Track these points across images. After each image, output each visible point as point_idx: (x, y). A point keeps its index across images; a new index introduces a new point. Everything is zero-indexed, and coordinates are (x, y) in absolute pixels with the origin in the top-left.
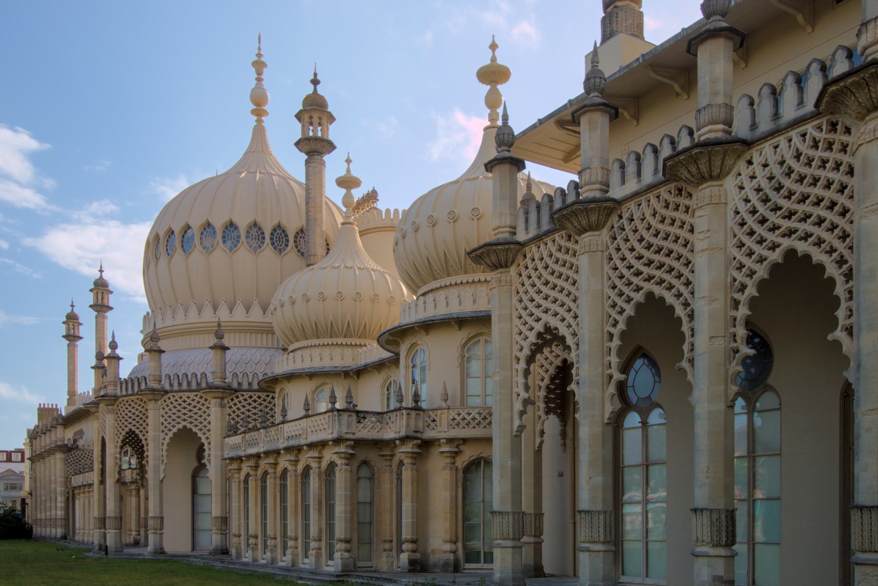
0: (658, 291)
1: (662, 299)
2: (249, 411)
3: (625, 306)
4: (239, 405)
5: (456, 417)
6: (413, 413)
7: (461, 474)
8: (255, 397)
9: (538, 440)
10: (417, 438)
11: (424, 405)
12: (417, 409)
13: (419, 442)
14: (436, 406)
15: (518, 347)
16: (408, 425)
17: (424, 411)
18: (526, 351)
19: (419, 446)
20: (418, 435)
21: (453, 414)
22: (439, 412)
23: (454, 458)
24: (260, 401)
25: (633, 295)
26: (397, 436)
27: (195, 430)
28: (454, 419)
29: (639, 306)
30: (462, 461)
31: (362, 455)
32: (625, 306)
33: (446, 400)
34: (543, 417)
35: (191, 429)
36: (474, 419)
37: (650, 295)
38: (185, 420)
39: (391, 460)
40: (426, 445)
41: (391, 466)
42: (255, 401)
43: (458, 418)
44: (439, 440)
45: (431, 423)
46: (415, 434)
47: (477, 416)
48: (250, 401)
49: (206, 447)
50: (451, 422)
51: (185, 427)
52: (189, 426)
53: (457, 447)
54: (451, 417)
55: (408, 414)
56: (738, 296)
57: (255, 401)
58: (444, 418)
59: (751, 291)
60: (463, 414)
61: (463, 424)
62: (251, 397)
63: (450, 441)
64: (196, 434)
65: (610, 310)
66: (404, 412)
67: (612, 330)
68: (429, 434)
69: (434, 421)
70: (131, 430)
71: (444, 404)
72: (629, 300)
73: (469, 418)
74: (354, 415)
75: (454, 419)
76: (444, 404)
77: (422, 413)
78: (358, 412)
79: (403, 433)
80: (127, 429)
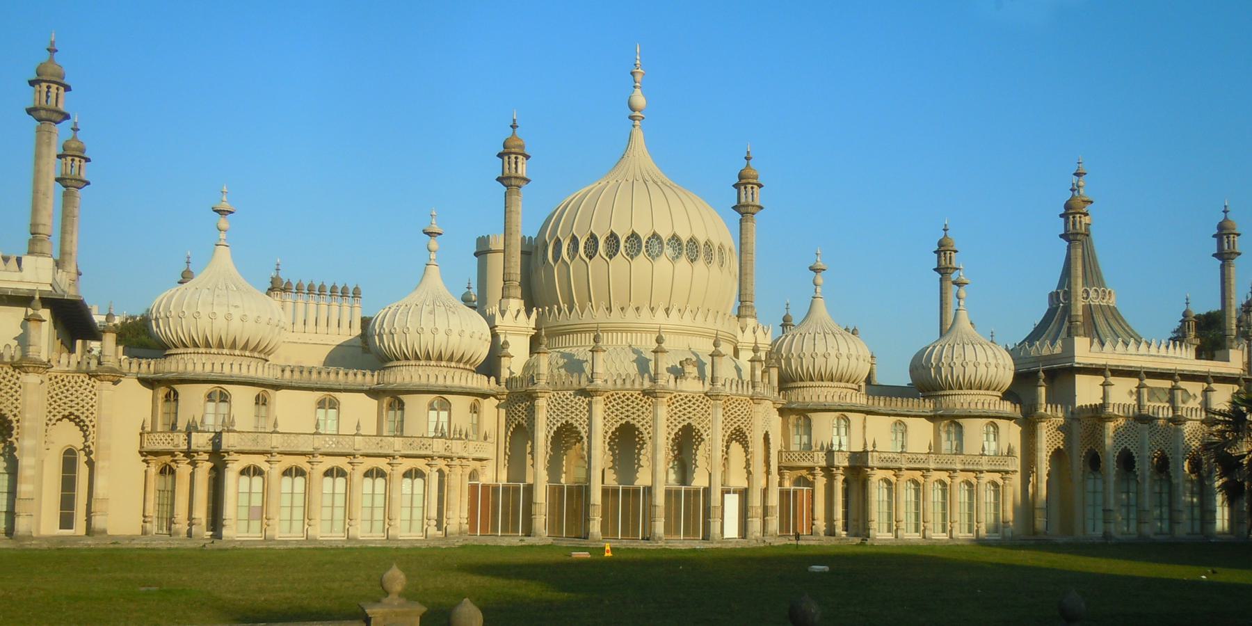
27: (576, 424)
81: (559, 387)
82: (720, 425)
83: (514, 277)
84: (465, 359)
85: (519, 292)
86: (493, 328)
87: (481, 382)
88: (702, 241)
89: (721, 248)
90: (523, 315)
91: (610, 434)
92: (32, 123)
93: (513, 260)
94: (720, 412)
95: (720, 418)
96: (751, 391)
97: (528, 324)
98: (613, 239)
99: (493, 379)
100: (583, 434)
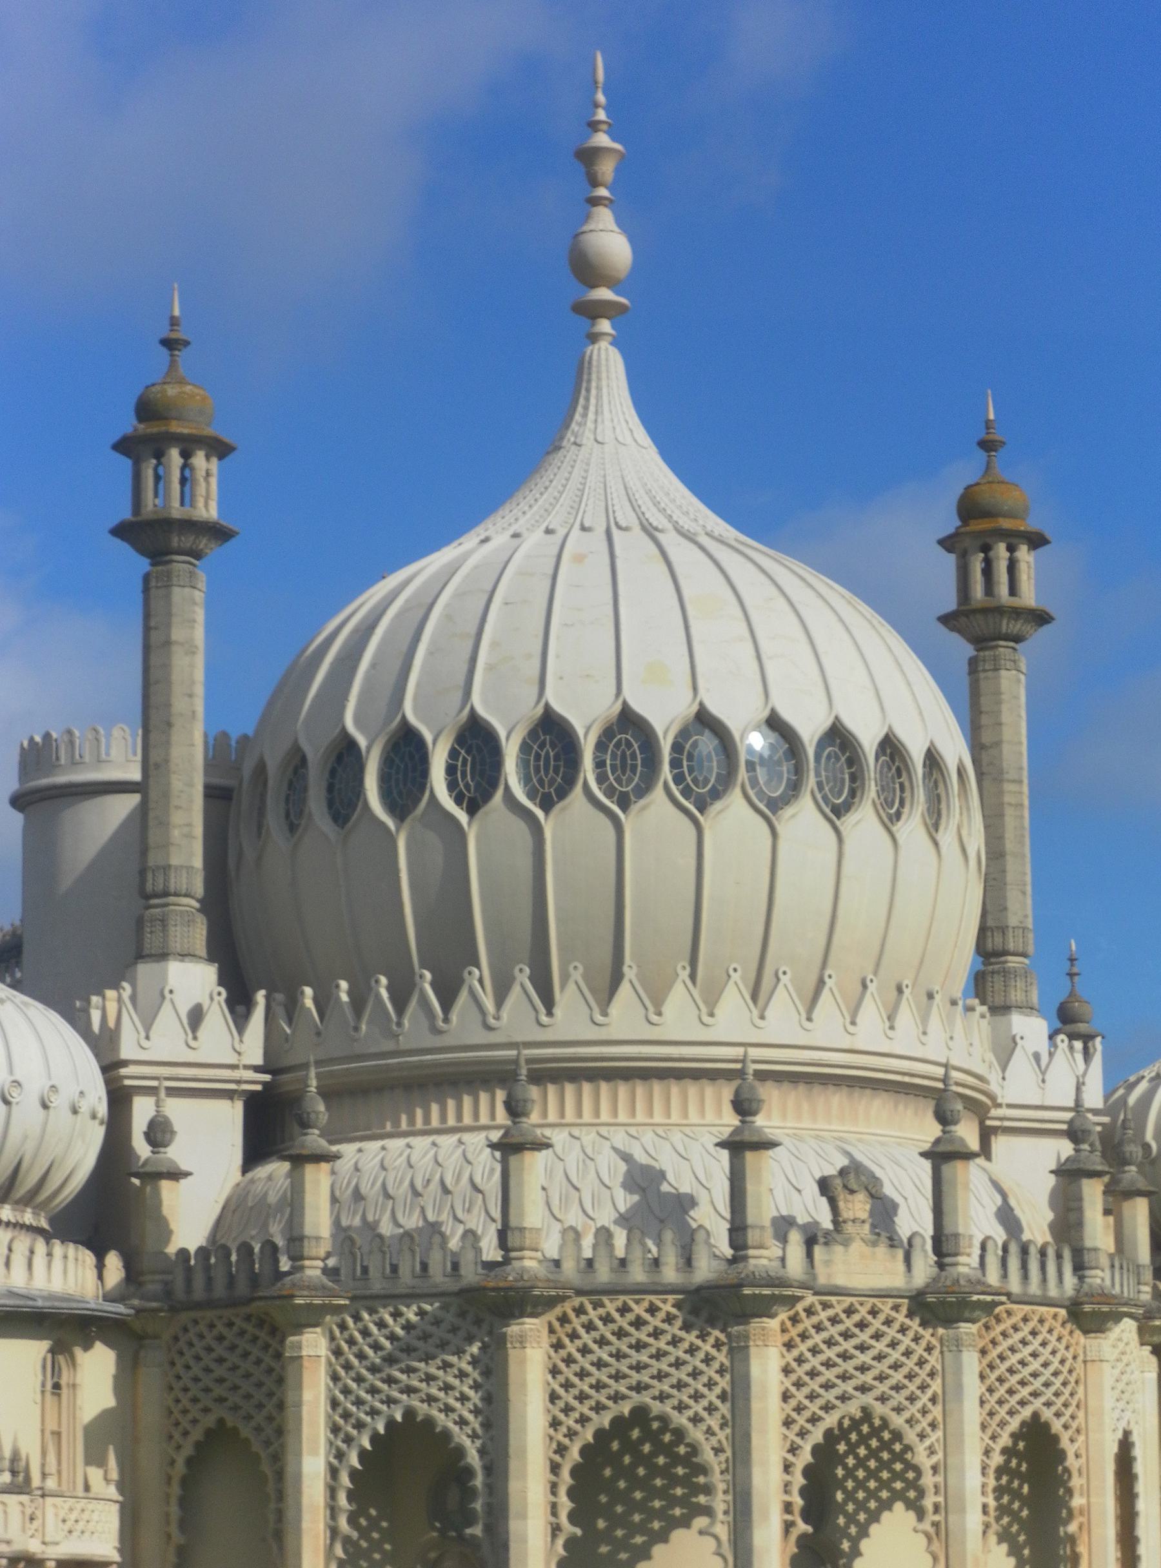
2: (619, 1356)
4: (587, 1338)
8: (639, 1310)
24: (656, 1322)
35: (429, 1422)
38: (409, 1390)
42: (638, 1323)
48: (623, 1322)
49: (479, 1481)
51: (409, 1413)
52: (422, 1409)
57: (638, 1323)
62: (624, 1310)
64: (446, 1435)
70: (221, 1422)
80: (209, 1421)
81: (377, 1285)
82: (971, 1414)
83: (177, 882)
84: (21, 1190)
85: (199, 934)
86: (110, 1068)
87: (71, 1276)
88: (868, 739)
89: (933, 759)
90: (217, 1018)
91: (574, 1454)
92: (164, 351)
93: (177, 818)
94: (971, 1363)
95: (973, 1388)
96: (1070, 1280)
97: (237, 1049)
98: (552, 735)
99: (114, 1262)
100: (473, 1458)
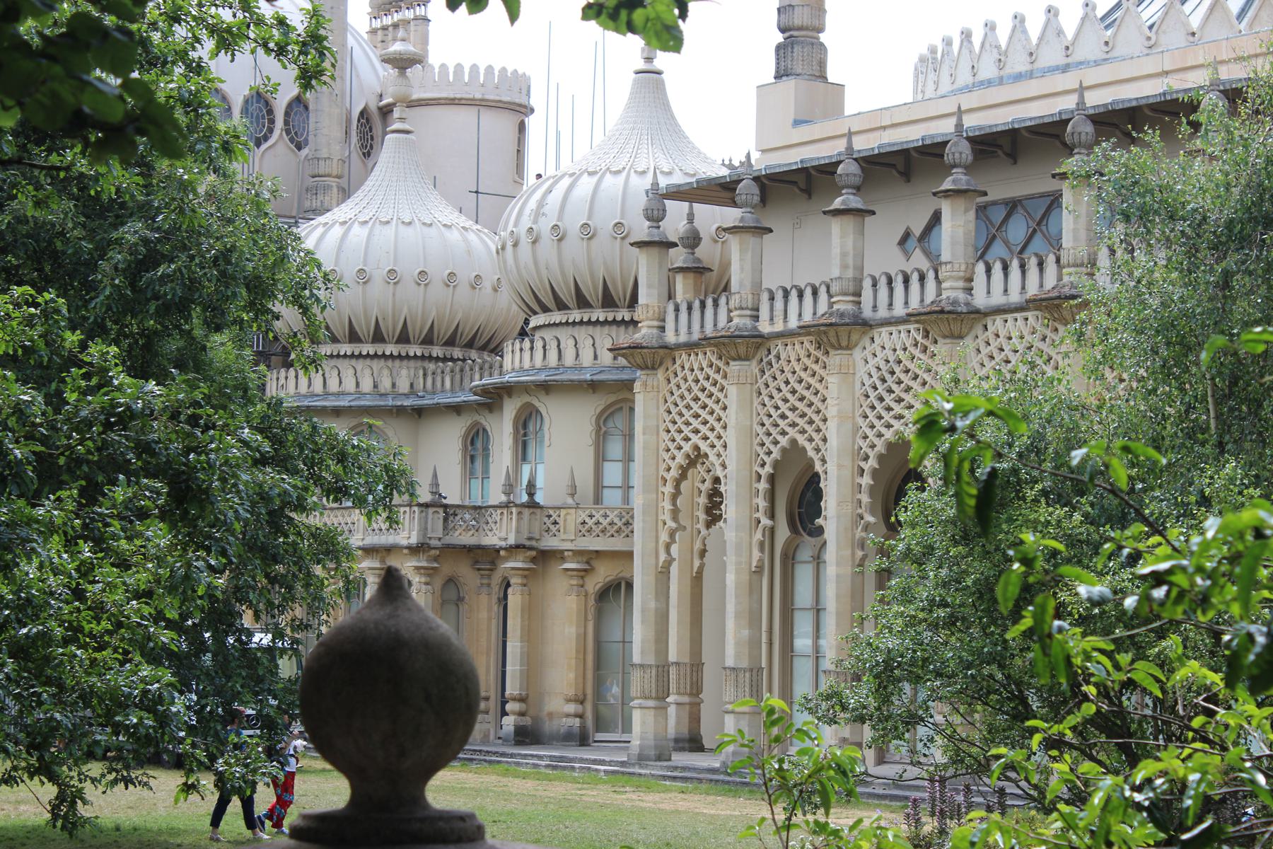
0: (801, 440)
1: (804, 449)
3: (772, 448)
5: (587, 520)
6: (526, 512)
7: (592, 602)
9: (697, 563)
10: (531, 548)
11: (539, 498)
12: (533, 505)
13: (534, 553)
14: (558, 503)
15: (664, 466)
16: (518, 532)
17: (541, 507)
18: (674, 473)
19: (533, 560)
20: (534, 543)
21: (583, 516)
22: (563, 512)
23: (582, 577)
25: (779, 438)
26: (503, 544)
28: (584, 523)
29: (784, 450)
30: (595, 583)
31: (447, 569)
32: (772, 448)
33: (572, 495)
34: (704, 532)
36: (612, 524)
37: (794, 442)
39: (489, 577)
40: (544, 558)
41: (489, 585)
43: (590, 522)
44: (562, 552)
45: (552, 527)
46: (528, 543)
47: (616, 520)
50: (580, 527)
53: (588, 563)
54: (580, 520)
55: (519, 513)
56: (862, 464)
58: (570, 520)
59: (873, 462)
60: (598, 516)
61: (597, 530)
63: (578, 553)
65: (759, 449)
66: (514, 510)
67: (760, 470)
68: (550, 543)
69: (555, 523)
71: (570, 501)
72: (776, 443)
73: (605, 522)
74: (441, 510)
75: (584, 523)
76: (570, 501)
77: (538, 511)
78: (446, 506)
79: (512, 541)
